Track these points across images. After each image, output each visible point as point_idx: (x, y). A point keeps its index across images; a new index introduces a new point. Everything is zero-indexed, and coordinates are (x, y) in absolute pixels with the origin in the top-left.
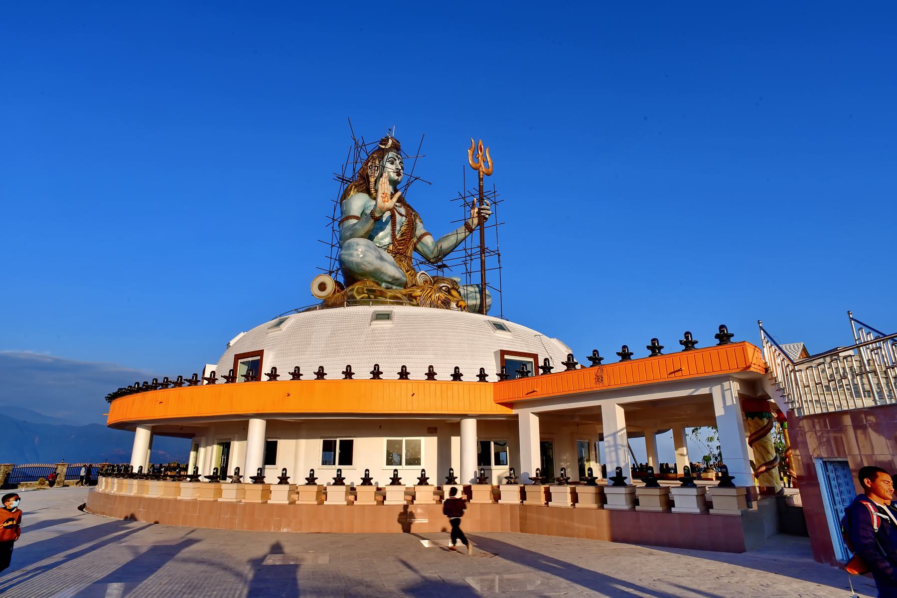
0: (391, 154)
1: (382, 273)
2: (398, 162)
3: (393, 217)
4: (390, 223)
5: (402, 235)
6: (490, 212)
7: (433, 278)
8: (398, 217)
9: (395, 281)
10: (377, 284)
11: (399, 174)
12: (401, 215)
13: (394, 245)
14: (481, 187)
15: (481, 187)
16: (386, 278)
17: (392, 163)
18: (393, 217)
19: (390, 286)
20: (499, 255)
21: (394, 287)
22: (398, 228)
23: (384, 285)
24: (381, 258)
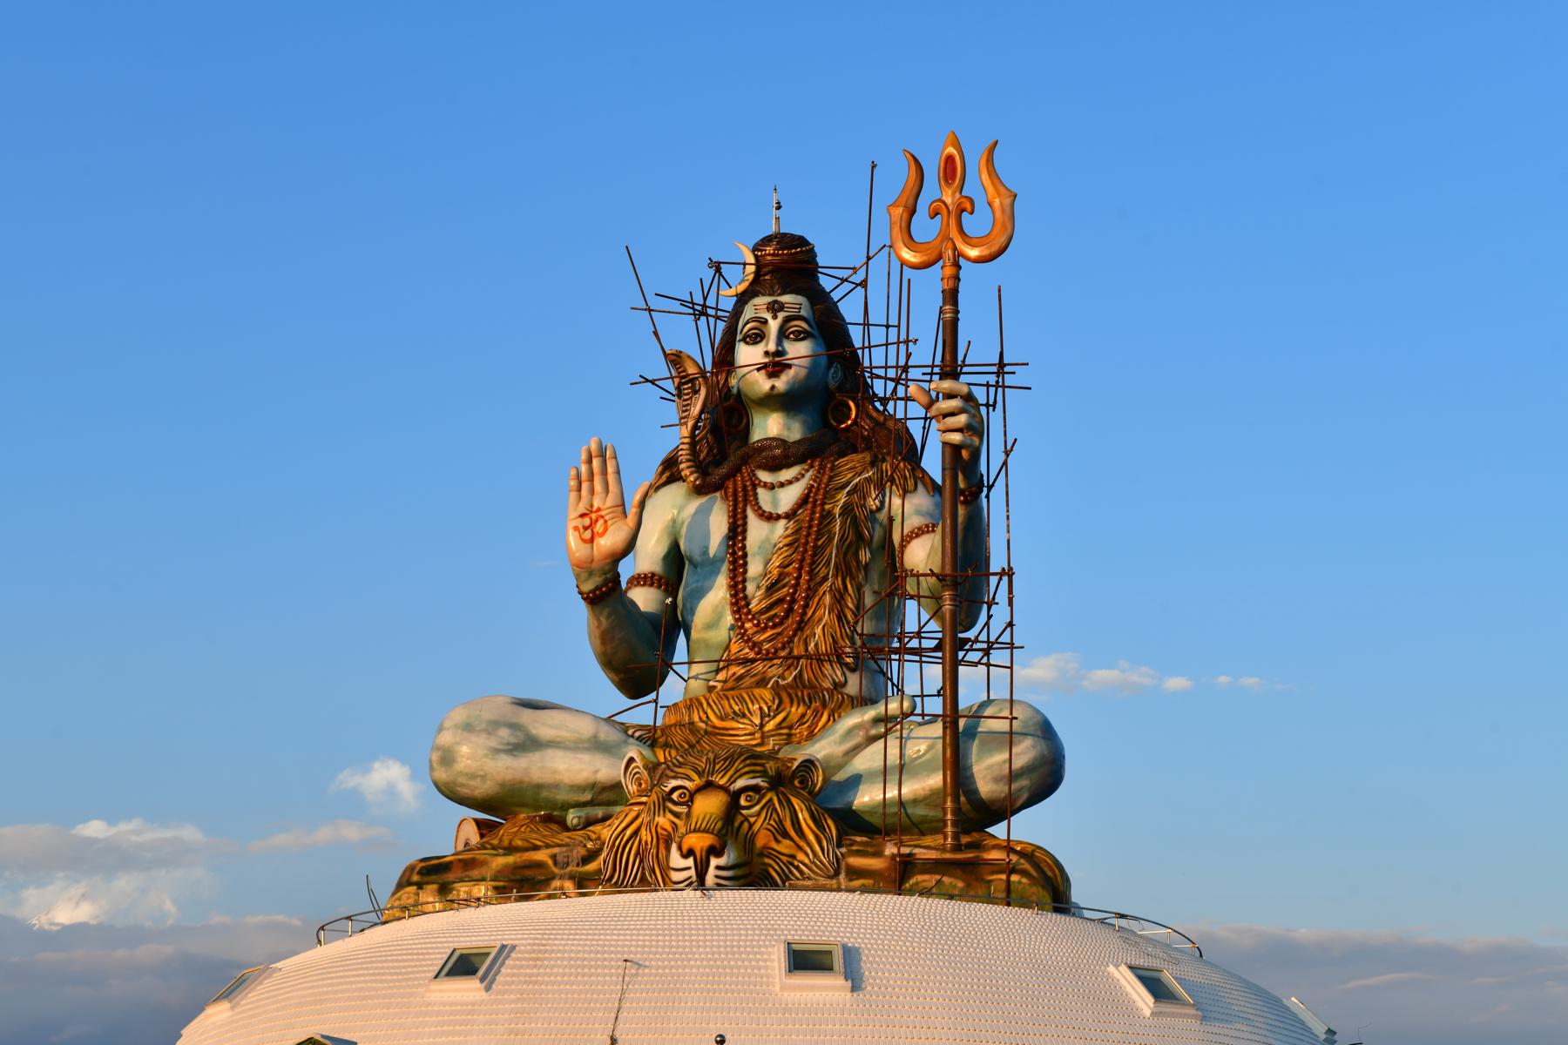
0: (749, 312)
1: (539, 787)
2: (774, 325)
3: (737, 531)
4: (725, 567)
5: (771, 589)
6: (962, 419)
7: (652, 768)
8: (757, 532)
9: (607, 796)
10: (548, 819)
11: (775, 366)
12: (770, 518)
13: (744, 637)
14: (951, 329)
15: (951, 329)
16: (562, 796)
17: (757, 337)
18: (737, 531)
19: (599, 812)
20: (1008, 573)
21: (618, 809)
22: (754, 568)
23: (572, 817)
24: (528, 744)
